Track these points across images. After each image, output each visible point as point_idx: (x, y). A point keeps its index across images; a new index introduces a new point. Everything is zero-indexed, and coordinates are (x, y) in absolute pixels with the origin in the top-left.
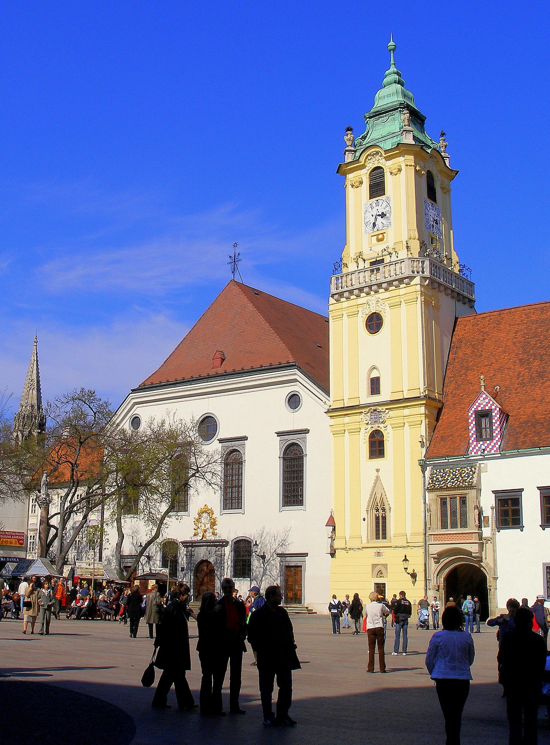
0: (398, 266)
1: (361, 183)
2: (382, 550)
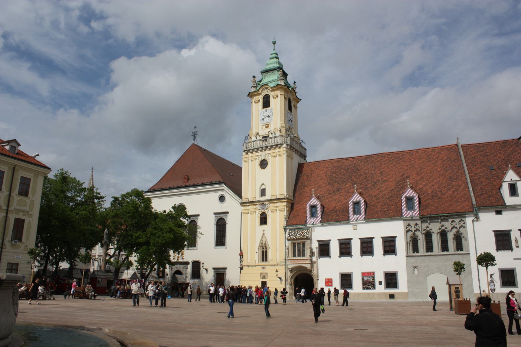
0: (276, 139)
1: (259, 101)
2: (265, 267)
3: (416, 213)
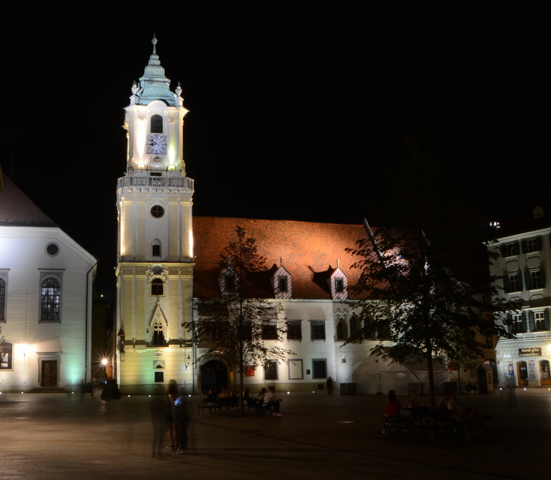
3: (344, 296)
